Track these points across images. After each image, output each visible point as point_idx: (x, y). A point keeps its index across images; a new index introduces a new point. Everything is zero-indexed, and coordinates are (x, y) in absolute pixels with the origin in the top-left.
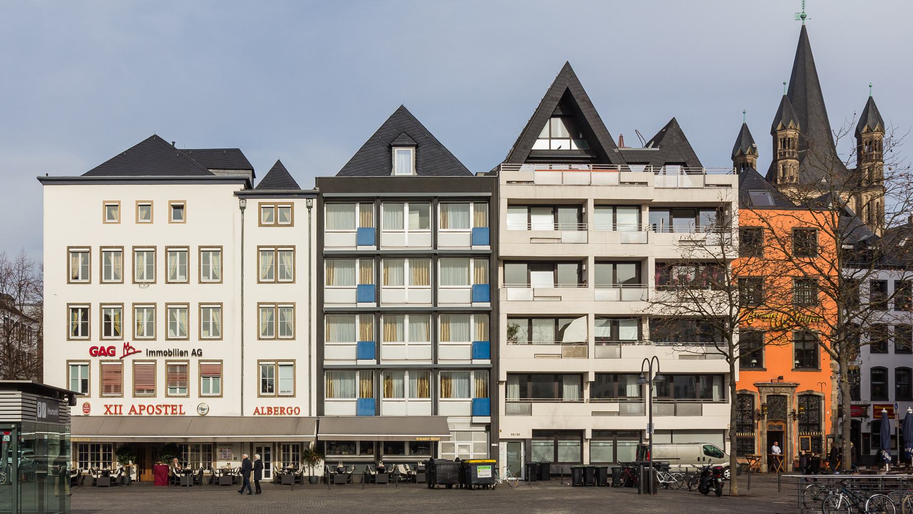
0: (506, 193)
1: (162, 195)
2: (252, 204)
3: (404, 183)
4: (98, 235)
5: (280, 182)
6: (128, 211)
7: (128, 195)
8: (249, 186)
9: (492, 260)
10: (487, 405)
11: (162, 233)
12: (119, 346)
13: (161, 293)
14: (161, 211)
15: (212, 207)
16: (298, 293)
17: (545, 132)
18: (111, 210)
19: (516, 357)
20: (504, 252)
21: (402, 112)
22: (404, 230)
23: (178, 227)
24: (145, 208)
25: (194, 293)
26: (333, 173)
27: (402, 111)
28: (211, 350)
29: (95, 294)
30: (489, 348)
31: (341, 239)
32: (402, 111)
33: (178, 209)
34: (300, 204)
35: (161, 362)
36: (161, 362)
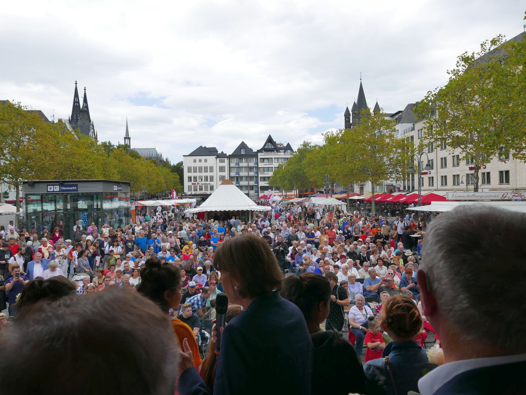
0: (259, 157)
1: (203, 158)
2: (218, 159)
3: (243, 155)
4: (193, 165)
5: (222, 156)
6: (198, 161)
7: (197, 158)
8: (217, 156)
9: (257, 168)
10: (257, 192)
11: (203, 164)
13: (203, 174)
14: (203, 161)
15: (212, 160)
16: (226, 174)
18: (195, 161)
19: (262, 184)
21: (243, 143)
23: (206, 163)
24: (200, 161)
25: (209, 174)
27: (243, 142)
28: (212, 183)
29: (192, 174)
31: (233, 165)
32: (243, 143)
33: (206, 161)
34: (226, 159)
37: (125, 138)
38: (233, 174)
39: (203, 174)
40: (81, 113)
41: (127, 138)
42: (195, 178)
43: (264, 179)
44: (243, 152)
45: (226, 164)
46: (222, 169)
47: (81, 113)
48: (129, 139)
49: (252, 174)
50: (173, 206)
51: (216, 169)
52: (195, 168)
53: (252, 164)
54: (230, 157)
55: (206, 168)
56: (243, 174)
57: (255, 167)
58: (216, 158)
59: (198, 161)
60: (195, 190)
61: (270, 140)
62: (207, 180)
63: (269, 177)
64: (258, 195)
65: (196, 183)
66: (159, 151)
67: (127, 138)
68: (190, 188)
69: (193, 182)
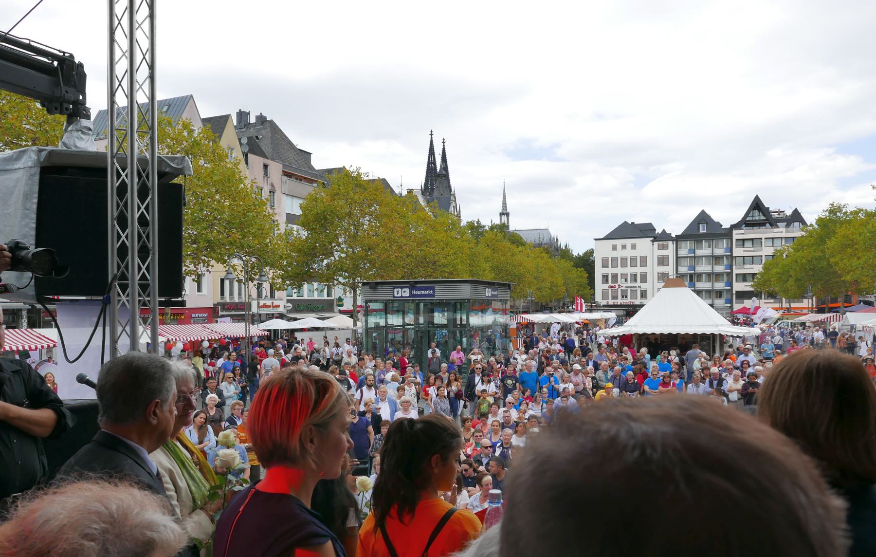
0: (735, 237)
1: (628, 242)
2: (656, 243)
3: (703, 235)
5: (663, 238)
6: (619, 247)
7: (619, 243)
8: (655, 238)
9: (731, 257)
10: (730, 301)
11: (629, 253)
12: (617, 285)
13: (629, 270)
14: (629, 247)
15: (644, 246)
16: (670, 269)
17: (751, 214)
18: (614, 248)
19: (739, 286)
20: (734, 255)
21: (703, 213)
22: (704, 250)
23: (633, 251)
25: (639, 270)
26: (680, 233)
27: (703, 212)
28: (644, 286)
29: (610, 271)
30: (730, 284)
31: (683, 253)
32: (703, 212)
33: (634, 247)
34: (670, 243)
35: (629, 290)
36: (629, 290)
37: (501, 214)
38: (683, 269)
39: (629, 270)
40: (437, 177)
41: (505, 213)
42: (615, 277)
43: (744, 277)
44: (702, 230)
45: (670, 251)
46: (663, 261)
47: (437, 177)
48: (507, 214)
49: (720, 268)
50: (577, 323)
51: (652, 262)
52: (614, 260)
53: (719, 251)
54: (679, 239)
55: (634, 260)
56: (703, 268)
57: (727, 256)
58: (653, 241)
59: (619, 247)
60: (615, 297)
61: (757, 205)
62: (636, 280)
63: (754, 275)
64: (731, 307)
65: (617, 285)
66: (554, 233)
67: (505, 213)
68: (605, 294)
69: (610, 284)
